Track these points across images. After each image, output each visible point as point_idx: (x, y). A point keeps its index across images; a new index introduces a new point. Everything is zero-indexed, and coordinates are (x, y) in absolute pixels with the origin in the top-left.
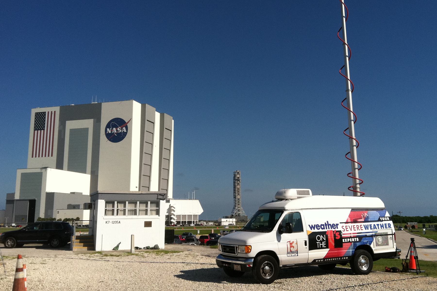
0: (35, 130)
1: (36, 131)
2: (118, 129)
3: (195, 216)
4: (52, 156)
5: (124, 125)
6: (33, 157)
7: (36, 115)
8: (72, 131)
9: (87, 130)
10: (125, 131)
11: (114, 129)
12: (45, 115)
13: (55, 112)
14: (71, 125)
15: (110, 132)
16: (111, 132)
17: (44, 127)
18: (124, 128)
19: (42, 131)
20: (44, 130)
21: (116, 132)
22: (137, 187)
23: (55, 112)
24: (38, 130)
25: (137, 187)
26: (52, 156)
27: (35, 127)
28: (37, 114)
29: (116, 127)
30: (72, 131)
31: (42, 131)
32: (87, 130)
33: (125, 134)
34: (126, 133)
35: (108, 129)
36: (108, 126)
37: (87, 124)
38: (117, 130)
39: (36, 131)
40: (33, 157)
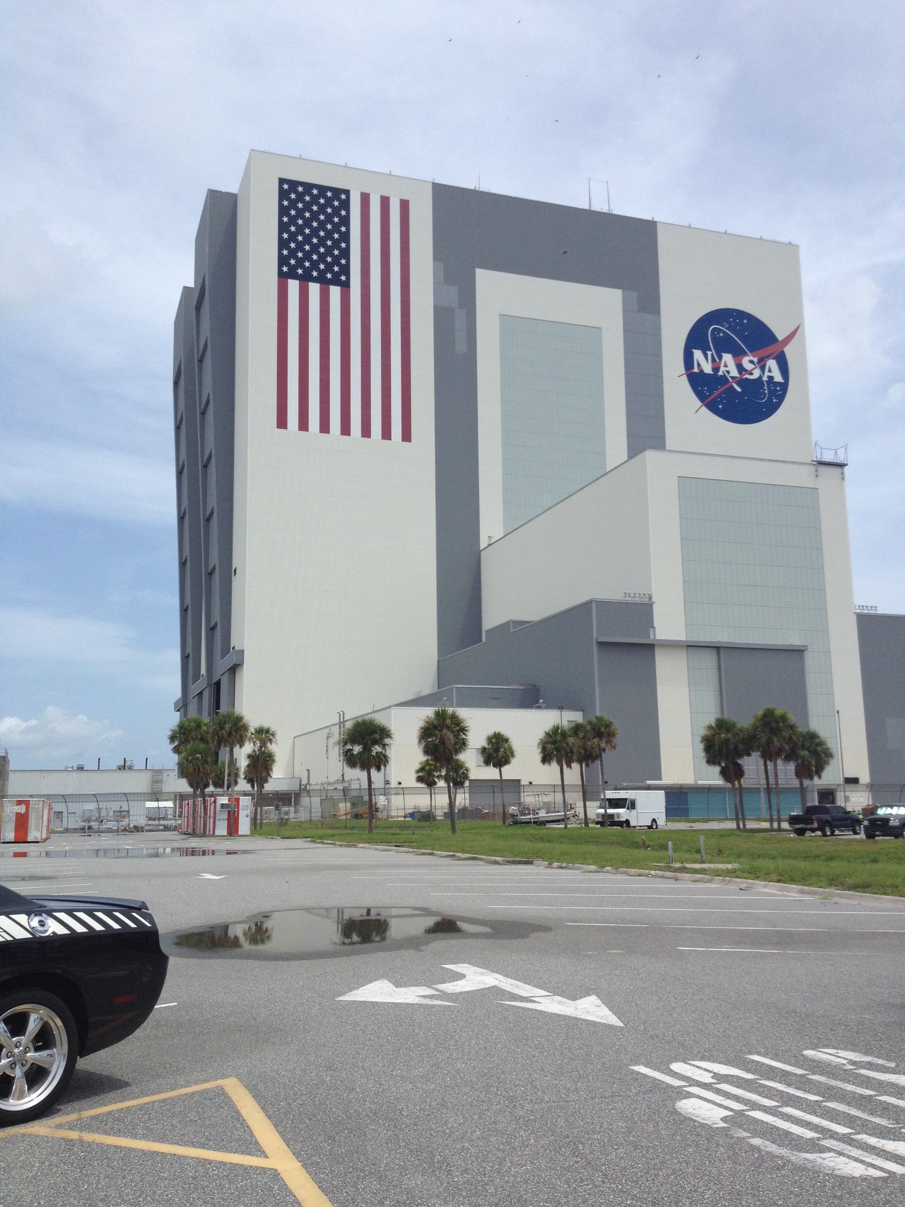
1: (293, 286)
4: (407, 436)
5: (770, 349)
6: (282, 423)
7: (283, 195)
8: (508, 323)
10: (778, 378)
11: (727, 358)
12: (346, 205)
13: (405, 205)
14: (500, 293)
15: (708, 369)
16: (716, 369)
17: (346, 270)
18: (772, 364)
20: (345, 286)
21: (734, 373)
23: (405, 205)
24: (305, 279)
26: (407, 436)
27: (282, 260)
29: (738, 354)
30: (508, 323)
31: (335, 292)
34: (784, 386)
35: (698, 354)
38: (740, 368)
40: (282, 423)
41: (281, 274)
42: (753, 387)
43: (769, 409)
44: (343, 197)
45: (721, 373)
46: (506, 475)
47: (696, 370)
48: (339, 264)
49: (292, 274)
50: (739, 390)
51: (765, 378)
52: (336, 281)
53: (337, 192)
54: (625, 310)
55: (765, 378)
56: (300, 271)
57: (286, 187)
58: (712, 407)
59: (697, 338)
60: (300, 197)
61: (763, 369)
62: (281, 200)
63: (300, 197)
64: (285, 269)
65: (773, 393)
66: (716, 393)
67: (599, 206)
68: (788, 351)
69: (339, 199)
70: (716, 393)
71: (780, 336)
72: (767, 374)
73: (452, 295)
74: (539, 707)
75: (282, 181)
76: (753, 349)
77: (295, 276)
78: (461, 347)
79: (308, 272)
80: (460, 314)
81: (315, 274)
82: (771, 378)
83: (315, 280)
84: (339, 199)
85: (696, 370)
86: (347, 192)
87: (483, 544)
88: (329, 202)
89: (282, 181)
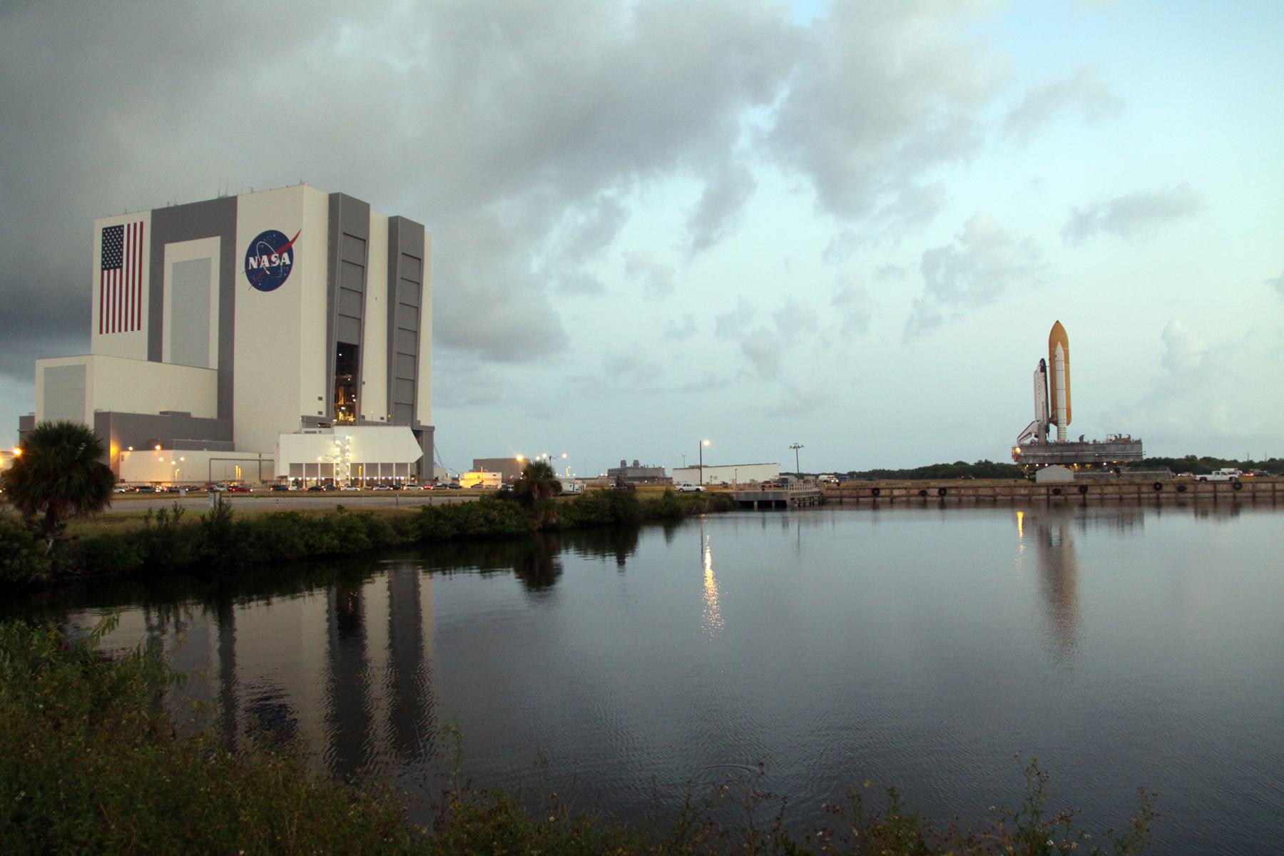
0: (103, 270)
2: (273, 259)
3: (402, 467)
8: (177, 266)
10: (288, 262)
11: (265, 258)
13: (142, 224)
15: (255, 266)
18: (285, 255)
20: (121, 268)
21: (267, 265)
22: (320, 399)
23: (142, 224)
24: (109, 270)
25: (320, 399)
32: (207, 261)
33: (287, 269)
34: (290, 266)
35: (251, 259)
36: (251, 252)
37: (210, 247)
42: (274, 270)
43: (283, 279)
67: (222, 194)
68: (293, 246)
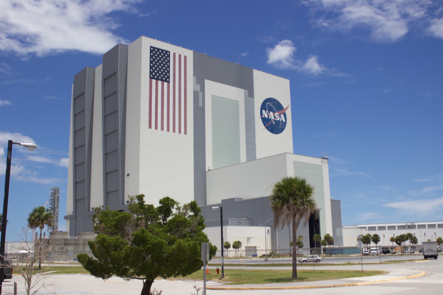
4: (185, 133)
6: (150, 127)
7: (151, 51)
8: (214, 98)
9: (236, 103)
11: (271, 113)
12: (169, 56)
13: (185, 57)
15: (266, 117)
16: (268, 117)
17: (169, 77)
18: (282, 116)
19: (166, 84)
20: (169, 82)
21: (273, 118)
23: (185, 57)
24: (157, 79)
26: (185, 133)
27: (151, 73)
28: (153, 50)
29: (274, 112)
30: (214, 98)
32: (236, 103)
34: (285, 123)
35: (264, 111)
39: (154, 81)
40: (150, 127)
41: (150, 77)
42: (277, 122)
43: (282, 130)
44: (168, 53)
45: (269, 118)
46: (213, 146)
47: (263, 116)
48: (167, 75)
49: (153, 78)
50: (274, 123)
51: (281, 120)
52: (166, 81)
53: (167, 52)
54: (245, 96)
55: (281, 120)
56: (156, 77)
57: (152, 49)
58: (267, 128)
59: (263, 107)
60: (156, 52)
61: (280, 117)
62: (151, 53)
63: (156, 52)
64: (151, 76)
65: (283, 125)
66: (269, 124)
69: (167, 54)
70: (269, 124)
71: (285, 107)
72: (281, 119)
73: (198, 86)
74: (260, 226)
75: (151, 47)
76: (278, 111)
77: (154, 78)
78: (201, 105)
79: (158, 77)
80: (201, 94)
81: (160, 78)
82: (282, 120)
83: (160, 80)
84: (167, 54)
85: (263, 116)
86: (169, 52)
87: (207, 170)
88: (164, 55)
89: (151, 47)
